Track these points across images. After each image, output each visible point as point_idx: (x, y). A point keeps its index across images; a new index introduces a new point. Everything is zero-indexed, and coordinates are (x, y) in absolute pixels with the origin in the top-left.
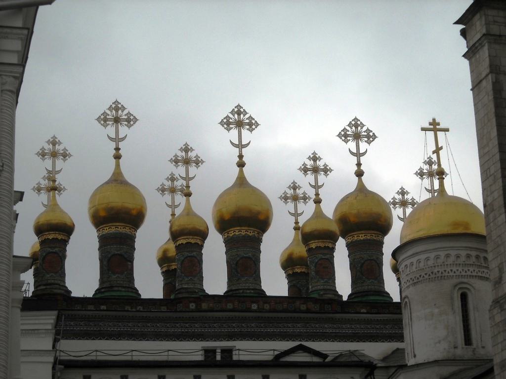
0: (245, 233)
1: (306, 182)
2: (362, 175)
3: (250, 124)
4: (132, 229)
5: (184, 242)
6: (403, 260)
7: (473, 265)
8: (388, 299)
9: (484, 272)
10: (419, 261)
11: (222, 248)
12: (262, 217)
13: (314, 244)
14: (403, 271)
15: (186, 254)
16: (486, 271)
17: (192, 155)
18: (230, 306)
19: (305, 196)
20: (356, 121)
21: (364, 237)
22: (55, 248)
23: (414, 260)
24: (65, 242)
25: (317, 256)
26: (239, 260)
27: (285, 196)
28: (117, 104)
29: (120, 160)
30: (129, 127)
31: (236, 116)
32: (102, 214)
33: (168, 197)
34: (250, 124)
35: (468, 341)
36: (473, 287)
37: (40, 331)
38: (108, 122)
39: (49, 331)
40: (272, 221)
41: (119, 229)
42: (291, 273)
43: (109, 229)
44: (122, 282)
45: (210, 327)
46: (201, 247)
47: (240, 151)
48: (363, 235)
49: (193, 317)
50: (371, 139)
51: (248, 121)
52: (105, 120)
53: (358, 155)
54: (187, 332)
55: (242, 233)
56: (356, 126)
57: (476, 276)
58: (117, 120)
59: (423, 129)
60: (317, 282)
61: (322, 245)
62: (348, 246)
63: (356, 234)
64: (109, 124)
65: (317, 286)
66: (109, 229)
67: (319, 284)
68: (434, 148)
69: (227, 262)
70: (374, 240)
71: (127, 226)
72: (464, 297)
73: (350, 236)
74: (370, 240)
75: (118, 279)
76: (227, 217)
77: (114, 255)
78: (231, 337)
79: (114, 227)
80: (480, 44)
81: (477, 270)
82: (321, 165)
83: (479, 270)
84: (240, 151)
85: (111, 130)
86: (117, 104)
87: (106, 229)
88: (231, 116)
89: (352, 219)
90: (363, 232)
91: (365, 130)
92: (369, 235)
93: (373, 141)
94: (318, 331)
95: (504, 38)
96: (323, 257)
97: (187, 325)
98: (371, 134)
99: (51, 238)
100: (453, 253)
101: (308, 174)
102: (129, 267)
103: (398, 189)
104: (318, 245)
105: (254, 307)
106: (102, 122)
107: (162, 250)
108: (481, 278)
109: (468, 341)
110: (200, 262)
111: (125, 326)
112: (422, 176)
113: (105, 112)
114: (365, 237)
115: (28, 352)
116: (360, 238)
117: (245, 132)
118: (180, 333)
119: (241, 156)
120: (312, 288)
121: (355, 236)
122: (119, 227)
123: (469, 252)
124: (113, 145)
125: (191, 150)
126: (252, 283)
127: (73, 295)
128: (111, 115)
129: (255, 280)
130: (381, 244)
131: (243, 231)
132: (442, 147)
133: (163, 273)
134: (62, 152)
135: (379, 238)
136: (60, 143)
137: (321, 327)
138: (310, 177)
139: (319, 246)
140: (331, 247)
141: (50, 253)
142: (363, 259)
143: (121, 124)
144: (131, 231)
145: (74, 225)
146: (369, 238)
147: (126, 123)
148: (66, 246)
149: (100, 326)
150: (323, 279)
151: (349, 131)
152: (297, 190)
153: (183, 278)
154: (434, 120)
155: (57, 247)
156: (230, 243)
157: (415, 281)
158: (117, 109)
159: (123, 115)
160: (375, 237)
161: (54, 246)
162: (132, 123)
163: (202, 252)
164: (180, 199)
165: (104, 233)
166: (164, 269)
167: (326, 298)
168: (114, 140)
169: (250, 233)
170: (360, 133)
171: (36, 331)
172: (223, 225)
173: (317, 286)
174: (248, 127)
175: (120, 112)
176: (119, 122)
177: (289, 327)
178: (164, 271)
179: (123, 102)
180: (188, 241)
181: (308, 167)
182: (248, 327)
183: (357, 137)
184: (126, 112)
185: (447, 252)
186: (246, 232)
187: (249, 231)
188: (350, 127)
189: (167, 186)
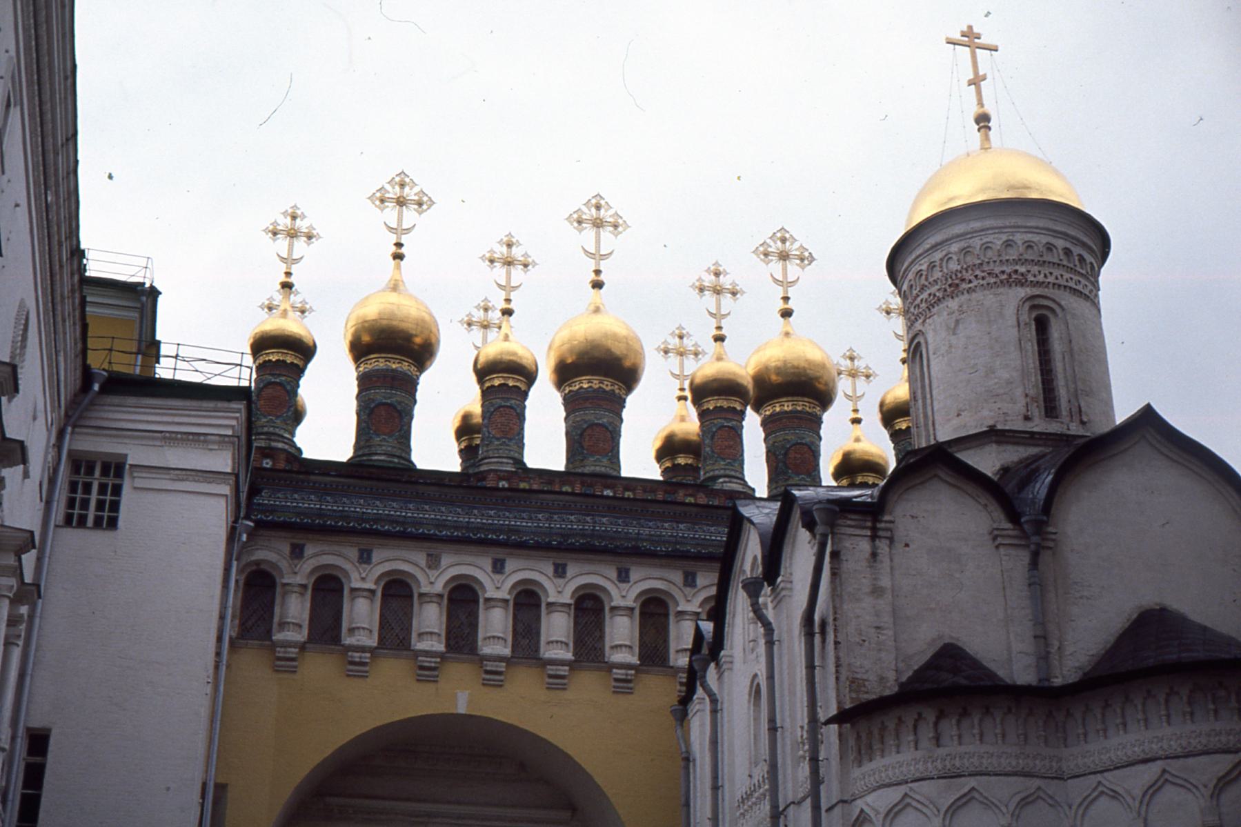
0: (597, 386)
5: (497, 383)
6: (912, 262)
7: (1059, 265)
9: (1079, 282)
12: (627, 363)
14: (911, 286)
15: (499, 402)
16: (1083, 281)
18: (566, 489)
21: (790, 408)
22: (279, 375)
23: (938, 256)
24: (299, 371)
25: (715, 421)
30: (420, 213)
32: (366, 338)
34: (616, 226)
36: (1059, 305)
37: (209, 437)
39: (226, 439)
40: (643, 370)
44: (389, 449)
45: (531, 518)
46: (525, 395)
47: (598, 264)
48: (790, 403)
50: (806, 262)
53: (785, 283)
54: (491, 524)
55: (593, 385)
56: (784, 240)
57: (1065, 287)
58: (401, 202)
60: (713, 464)
61: (725, 404)
62: (765, 424)
64: (388, 207)
69: (567, 434)
70: (808, 412)
72: (1042, 326)
73: (770, 405)
74: (800, 412)
75: (383, 443)
79: (383, 360)
81: (1067, 276)
82: (728, 283)
83: (1072, 276)
84: (598, 264)
85: (391, 214)
88: (585, 209)
90: (790, 399)
91: (797, 247)
94: (713, 538)
96: (725, 424)
97: (492, 513)
98: (806, 254)
99: (274, 360)
100: (1019, 238)
103: (844, 350)
105: (608, 493)
108: (1075, 291)
109: (1051, 410)
110: (521, 417)
112: (888, 313)
113: (383, 188)
115: (184, 472)
118: (479, 525)
120: (705, 474)
121: (777, 405)
122: (392, 361)
123: (1054, 241)
126: (606, 467)
127: (305, 455)
131: (595, 382)
132: (985, 75)
133: (461, 451)
134: (306, 231)
136: (303, 217)
137: (719, 533)
140: (739, 408)
141: (270, 383)
142: (789, 441)
143: (407, 207)
145: (315, 346)
147: (416, 207)
148: (300, 377)
149: (344, 503)
151: (771, 247)
155: (285, 376)
156: (572, 403)
161: (278, 372)
162: (425, 207)
163: (527, 403)
167: (727, 488)
168: (394, 231)
169: (607, 385)
171: (202, 438)
172: (565, 373)
173: (713, 470)
174: (611, 229)
175: (407, 189)
176: (405, 204)
177: (666, 529)
178: (463, 447)
182: (595, 522)
185: (1004, 237)
186: (601, 385)
187: (606, 383)
188: (773, 240)
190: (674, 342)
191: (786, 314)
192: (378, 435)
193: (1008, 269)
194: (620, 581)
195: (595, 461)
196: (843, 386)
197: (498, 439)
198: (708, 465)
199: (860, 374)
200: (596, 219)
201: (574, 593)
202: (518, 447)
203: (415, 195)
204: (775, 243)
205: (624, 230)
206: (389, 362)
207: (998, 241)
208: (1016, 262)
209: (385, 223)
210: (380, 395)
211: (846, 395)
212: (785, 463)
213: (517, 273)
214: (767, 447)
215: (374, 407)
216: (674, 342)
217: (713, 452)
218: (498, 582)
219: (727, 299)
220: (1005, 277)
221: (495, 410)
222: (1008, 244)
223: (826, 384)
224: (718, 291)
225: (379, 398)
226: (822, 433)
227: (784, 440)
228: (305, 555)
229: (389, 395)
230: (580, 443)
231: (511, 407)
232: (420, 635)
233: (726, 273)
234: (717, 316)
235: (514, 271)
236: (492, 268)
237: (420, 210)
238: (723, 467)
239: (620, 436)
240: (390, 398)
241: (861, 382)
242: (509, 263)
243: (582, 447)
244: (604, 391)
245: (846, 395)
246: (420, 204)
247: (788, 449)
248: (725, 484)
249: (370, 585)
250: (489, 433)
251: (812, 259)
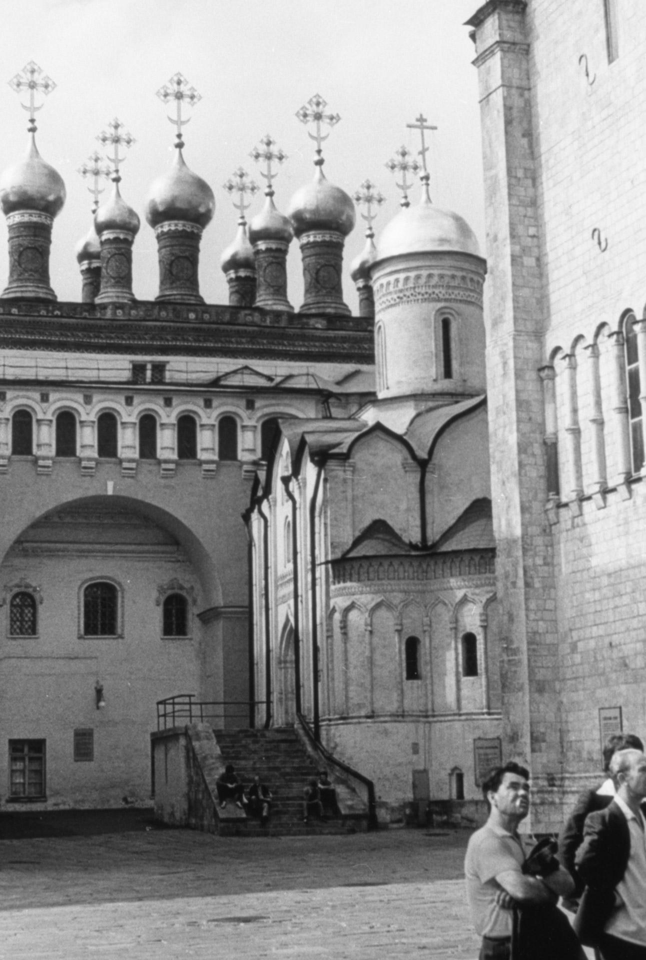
1: (255, 171)
3: (192, 97)
8: (347, 313)
10: (397, 281)
11: (154, 245)
16: (472, 294)
23: (392, 278)
32: (12, 198)
35: (448, 374)
53: (319, 139)
58: (32, 86)
59: (409, 126)
62: (303, 248)
68: (420, 149)
72: (446, 324)
76: (161, 208)
78: (165, 351)
80: (492, 51)
81: (462, 293)
89: (308, 216)
95: (518, 47)
105: (192, 316)
109: (448, 374)
128: (26, 78)
135: (340, 240)
138: (262, 162)
154: (421, 115)
157: (392, 302)
159: (38, 78)
164: (105, 183)
190: (236, 180)
191: (320, 163)
193: (430, 291)
196: (360, 209)
197: (114, 278)
207: (424, 273)
208: (435, 286)
211: (363, 216)
219: (275, 162)
220: (426, 296)
222: (430, 276)
224: (269, 157)
235: (119, 146)
241: (375, 205)
242: (117, 140)
245: (363, 216)
246: (46, 86)
249: (49, 416)
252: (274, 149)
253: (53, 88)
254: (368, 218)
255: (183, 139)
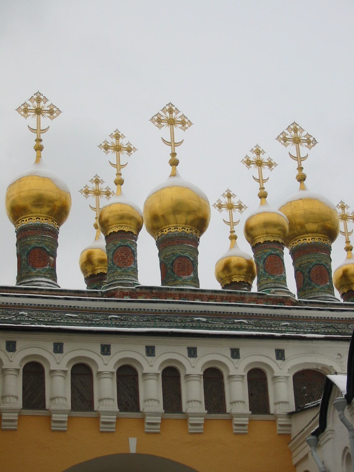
0: (181, 230)
2: (304, 179)
4: (55, 222)
5: (116, 230)
13: (262, 239)
15: (119, 243)
17: (123, 142)
19: (240, 205)
20: (295, 125)
21: (311, 241)
25: (265, 251)
26: (176, 259)
27: (220, 204)
28: (38, 95)
29: (42, 152)
31: (168, 114)
33: (92, 199)
34: (183, 123)
38: (29, 113)
41: (40, 221)
42: (229, 283)
43: (29, 220)
48: (310, 238)
49: (129, 309)
50: (311, 144)
51: (180, 120)
52: (26, 111)
53: (299, 159)
55: (178, 230)
58: (38, 112)
60: (267, 280)
62: (293, 253)
63: (301, 238)
65: (267, 284)
66: (29, 220)
67: (268, 281)
71: (50, 218)
73: (296, 240)
77: (35, 248)
85: (32, 120)
86: (38, 95)
87: (26, 220)
92: (317, 238)
93: (313, 146)
96: (273, 252)
98: (311, 139)
101: (251, 167)
102: (52, 263)
104: (267, 240)
106: (22, 113)
107: (86, 253)
110: (133, 254)
111: (49, 316)
114: (313, 240)
116: (307, 241)
117: (177, 129)
119: (174, 154)
121: (302, 239)
124: (34, 136)
125: (122, 137)
128: (33, 105)
129: (194, 282)
130: (328, 250)
131: (179, 228)
139: (268, 240)
142: (311, 263)
143: (43, 115)
144: (54, 224)
146: (317, 241)
147: (49, 115)
150: (273, 276)
152: (232, 198)
153: (116, 270)
158: (39, 100)
159: (45, 106)
160: (323, 240)
162: (55, 115)
165: (23, 225)
166: (89, 274)
169: (187, 230)
170: (300, 137)
173: (267, 284)
174: (180, 126)
175: (42, 103)
176: (41, 113)
178: (88, 276)
179: (45, 93)
180: (121, 229)
181: (251, 159)
183: (297, 141)
184: (48, 103)
186: (183, 230)
187: (187, 228)
188: (289, 131)
189: (91, 188)
192: (35, 269)
194: (232, 358)
195: (183, 281)
197: (121, 268)
198: (262, 281)
199: (348, 218)
200: (170, 119)
201: (203, 367)
202: (134, 273)
203: (48, 107)
204: (290, 133)
205: (189, 126)
206: (40, 219)
209: (28, 126)
210: (33, 241)
212: (310, 278)
213: (124, 157)
214: (295, 268)
215: (31, 250)
216: (224, 201)
217: (265, 271)
218: (151, 362)
219: (266, 170)
221: (116, 249)
223: (333, 224)
224: (259, 163)
225: (34, 244)
226: (332, 256)
227: (308, 262)
228: (17, 349)
229: (40, 242)
230: (172, 270)
231: (128, 246)
232: (100, 400)
233: (264, 152)
234: (261, 180)
236: (107, 154)
237: (52, 117)
238: (273, 281)
239: (198, 264)
240: (41, 243)
243: (174, 274)
244: (186, 234)
247: (311, 269)
248: (276, 293)
250: (113, 263)
251: (315, 142)
252: (264, 158)
253: (58, 115)
254: (347, 234)
255: (177, 157)
